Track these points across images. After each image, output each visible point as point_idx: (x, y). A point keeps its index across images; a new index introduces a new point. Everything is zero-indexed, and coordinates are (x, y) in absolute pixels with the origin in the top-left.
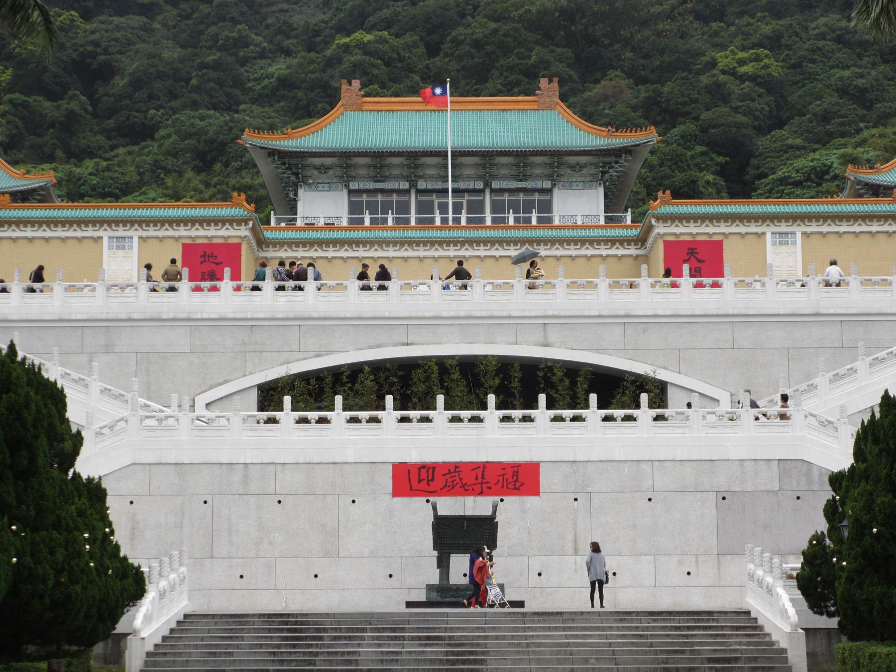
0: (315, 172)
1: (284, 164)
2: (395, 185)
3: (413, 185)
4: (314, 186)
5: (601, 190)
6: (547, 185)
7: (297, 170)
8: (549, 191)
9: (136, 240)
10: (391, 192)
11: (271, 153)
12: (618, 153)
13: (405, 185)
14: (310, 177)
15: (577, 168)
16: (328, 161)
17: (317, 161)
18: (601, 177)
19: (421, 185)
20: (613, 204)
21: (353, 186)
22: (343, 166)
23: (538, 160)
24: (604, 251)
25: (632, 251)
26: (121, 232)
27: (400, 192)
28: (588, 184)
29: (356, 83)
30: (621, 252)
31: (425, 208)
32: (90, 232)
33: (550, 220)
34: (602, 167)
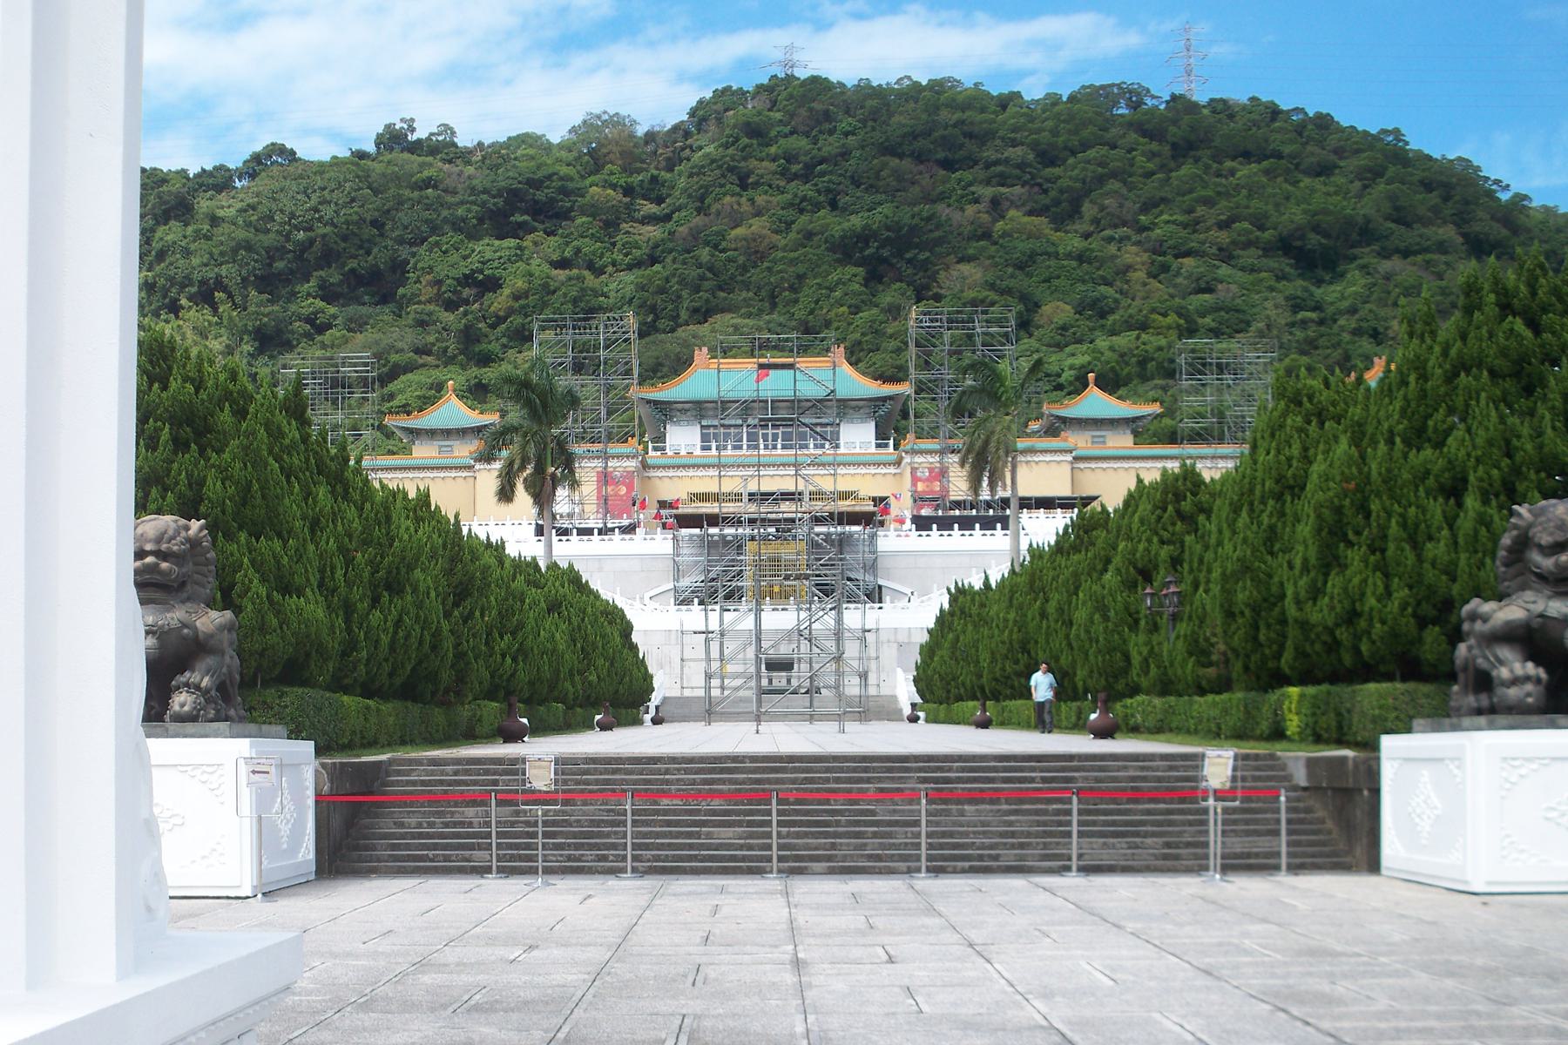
2: (733, 422)
3: (745, 420)
4: (678, 423)
7: (666, 412)
10: (729, 426)
11: (649, 402)
12: (884, 399)
15: (857, 409)
16: (687, 406)
18: (873, 414)
20: (881, 435)
21: (704, 423)
22: (698, 410)
24: (872, 470)
25: (892, 470)
27: (736, 426)
29: (705, 350)
30: (884, 471)
31: (752, 438)
33: (837, 446)
34: (872, 408)
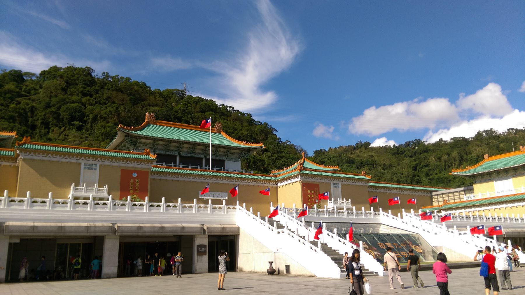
0: (141, 145)
1: (131, 140)
3: (179, 154)
5: (240, 162)
6: (224, 158)
8: (223, 162)
9: (98, 166)
12: (249, 150)
13: (176, 154)
14: (139, 147)
16: (148, 141)
17: (143, 141)
19: (182, 154)
23: (222, 150)
26: (91, 161)
28: (236, 160)
32: (74, 160)
